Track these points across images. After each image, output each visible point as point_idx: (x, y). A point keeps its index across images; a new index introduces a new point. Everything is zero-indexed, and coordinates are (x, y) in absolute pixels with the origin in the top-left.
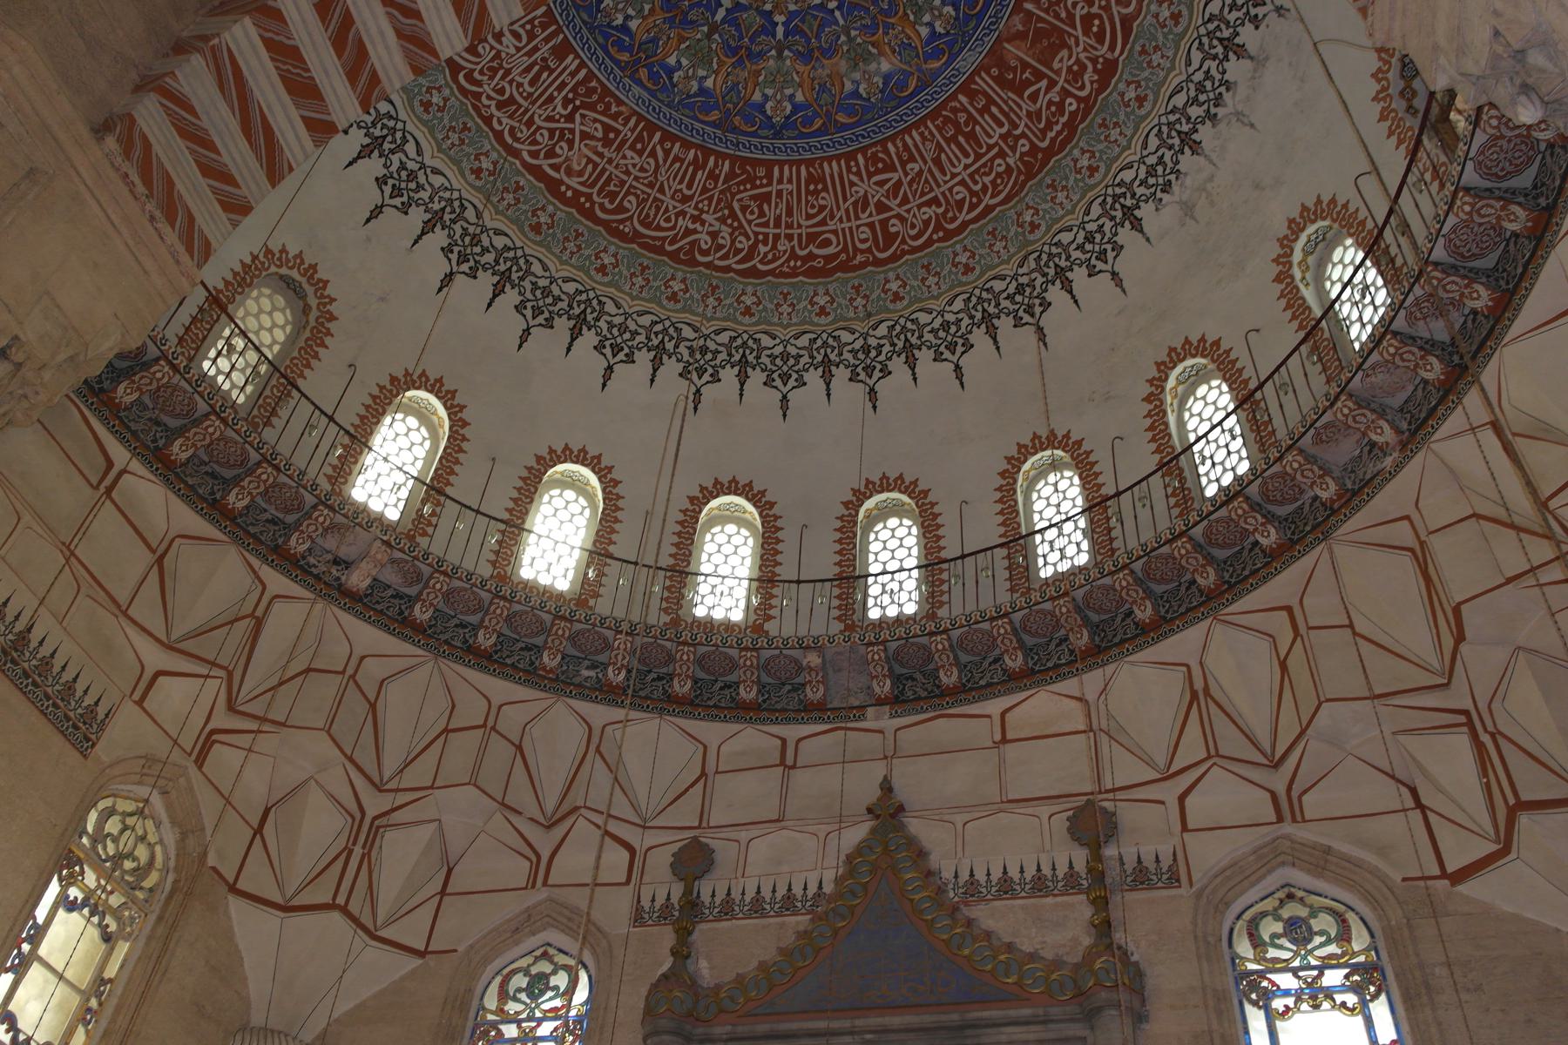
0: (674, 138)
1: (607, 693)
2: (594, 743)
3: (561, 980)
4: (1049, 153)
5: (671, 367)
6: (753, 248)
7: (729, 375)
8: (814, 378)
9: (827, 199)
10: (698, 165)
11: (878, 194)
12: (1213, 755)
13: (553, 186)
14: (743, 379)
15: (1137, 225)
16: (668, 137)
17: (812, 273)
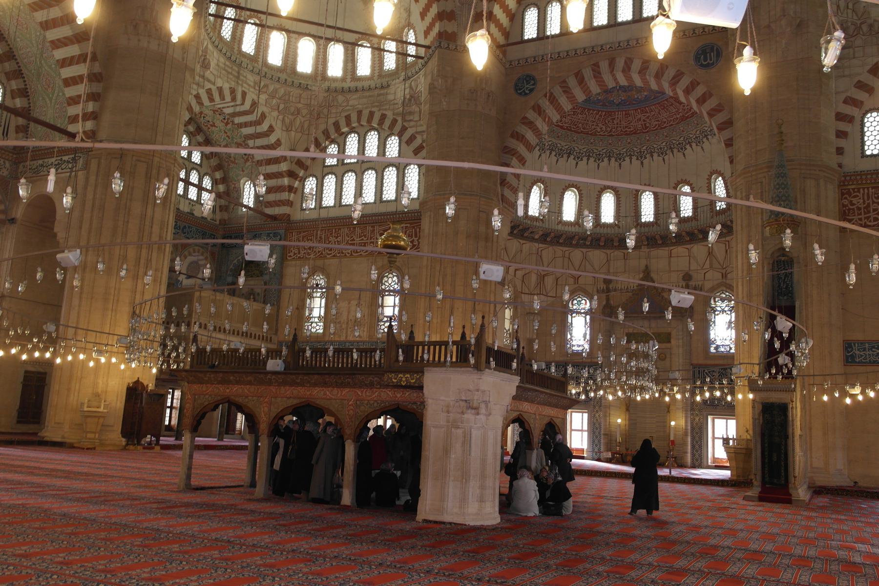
0: (589, 110)
1: (587, 247)
2: (585, 257)
3: (583, 302)
4: (687, 118)
5: (592, 160)
6: (611, 131)
7: (606, 160)
8: (627, 159)
9: (630, 118)
10: (597, 114)
11: (643, 118)
12: (711, 267)
13: (562, 127)
14: (609, 160)
15: (708, 139)
16: (589, 110)
17: (627, 134)
